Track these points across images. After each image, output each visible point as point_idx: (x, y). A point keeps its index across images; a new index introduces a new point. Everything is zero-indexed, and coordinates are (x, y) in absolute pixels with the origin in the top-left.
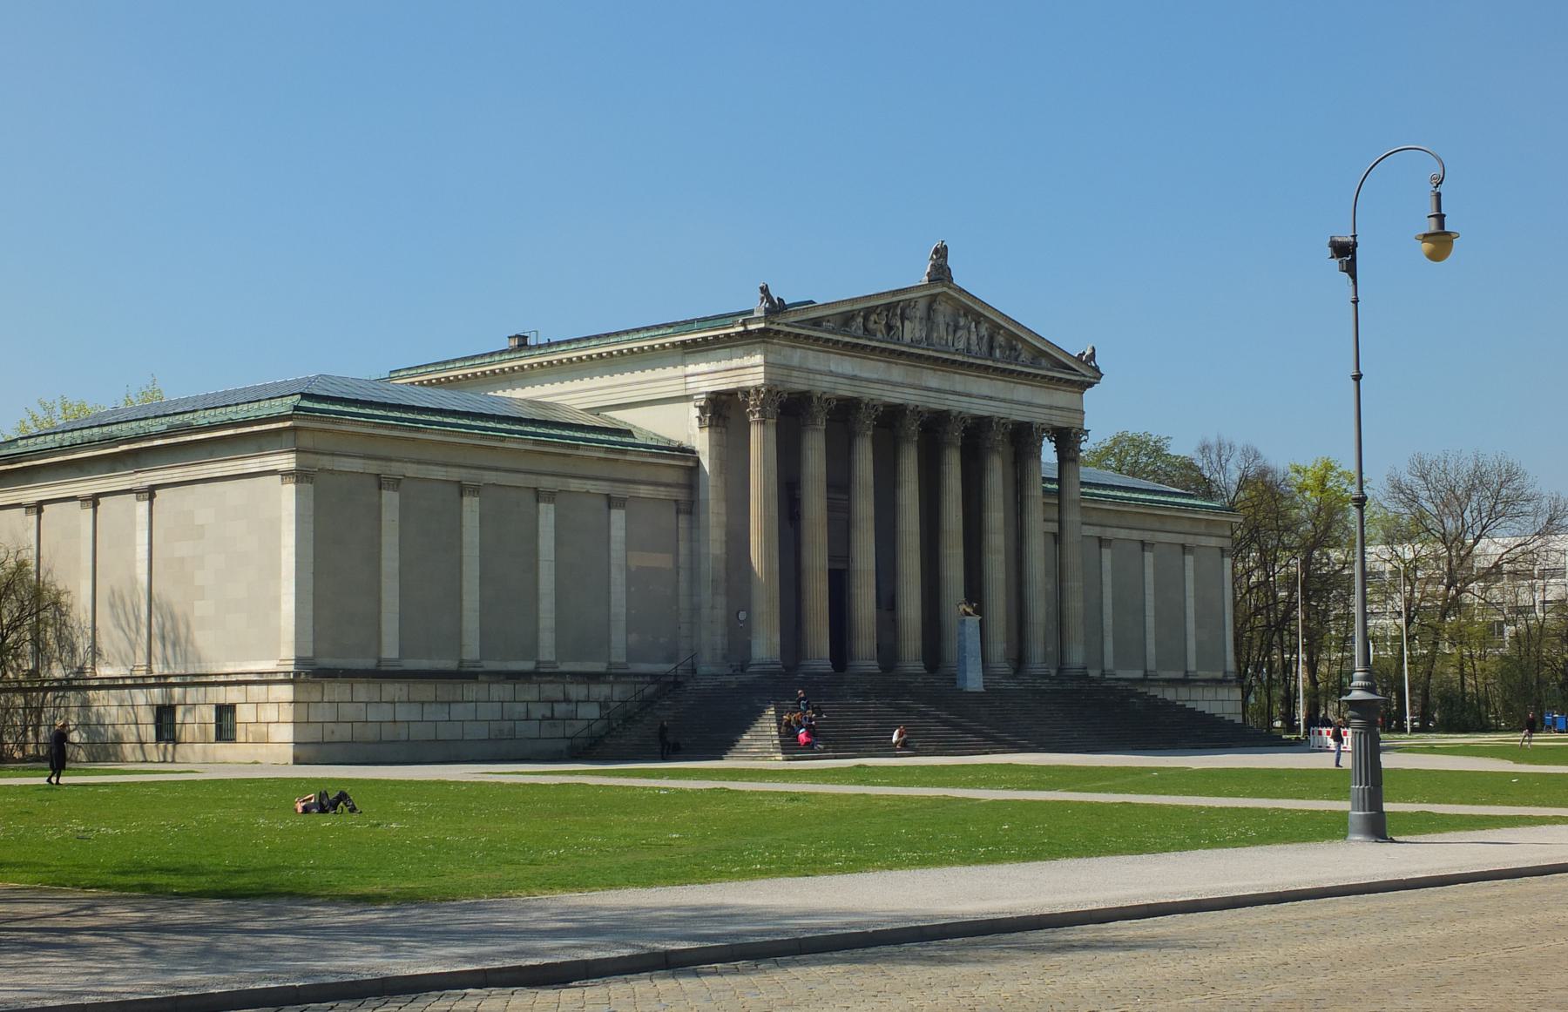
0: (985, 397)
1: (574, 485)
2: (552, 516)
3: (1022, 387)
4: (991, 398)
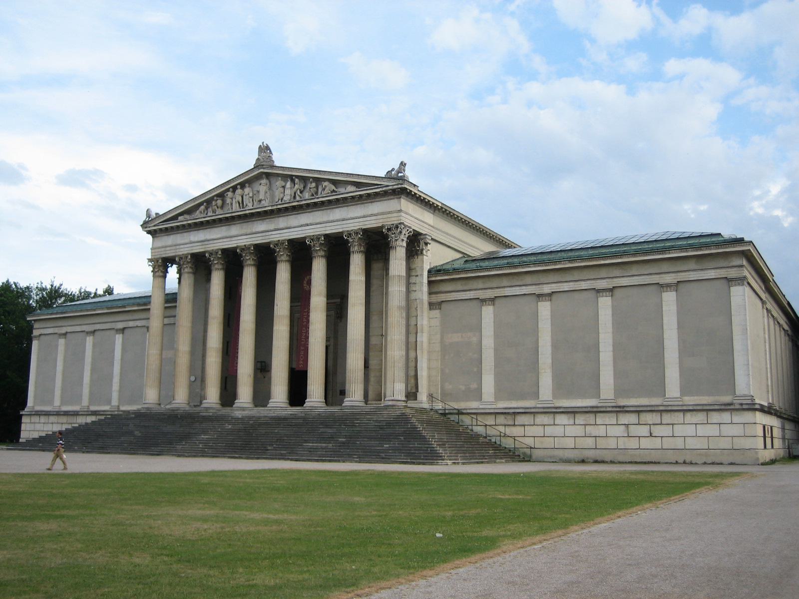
0: (302, 226)
1: (131, 324)
2: (121, 339)
3: (337, 210)
4: (307, 225)
